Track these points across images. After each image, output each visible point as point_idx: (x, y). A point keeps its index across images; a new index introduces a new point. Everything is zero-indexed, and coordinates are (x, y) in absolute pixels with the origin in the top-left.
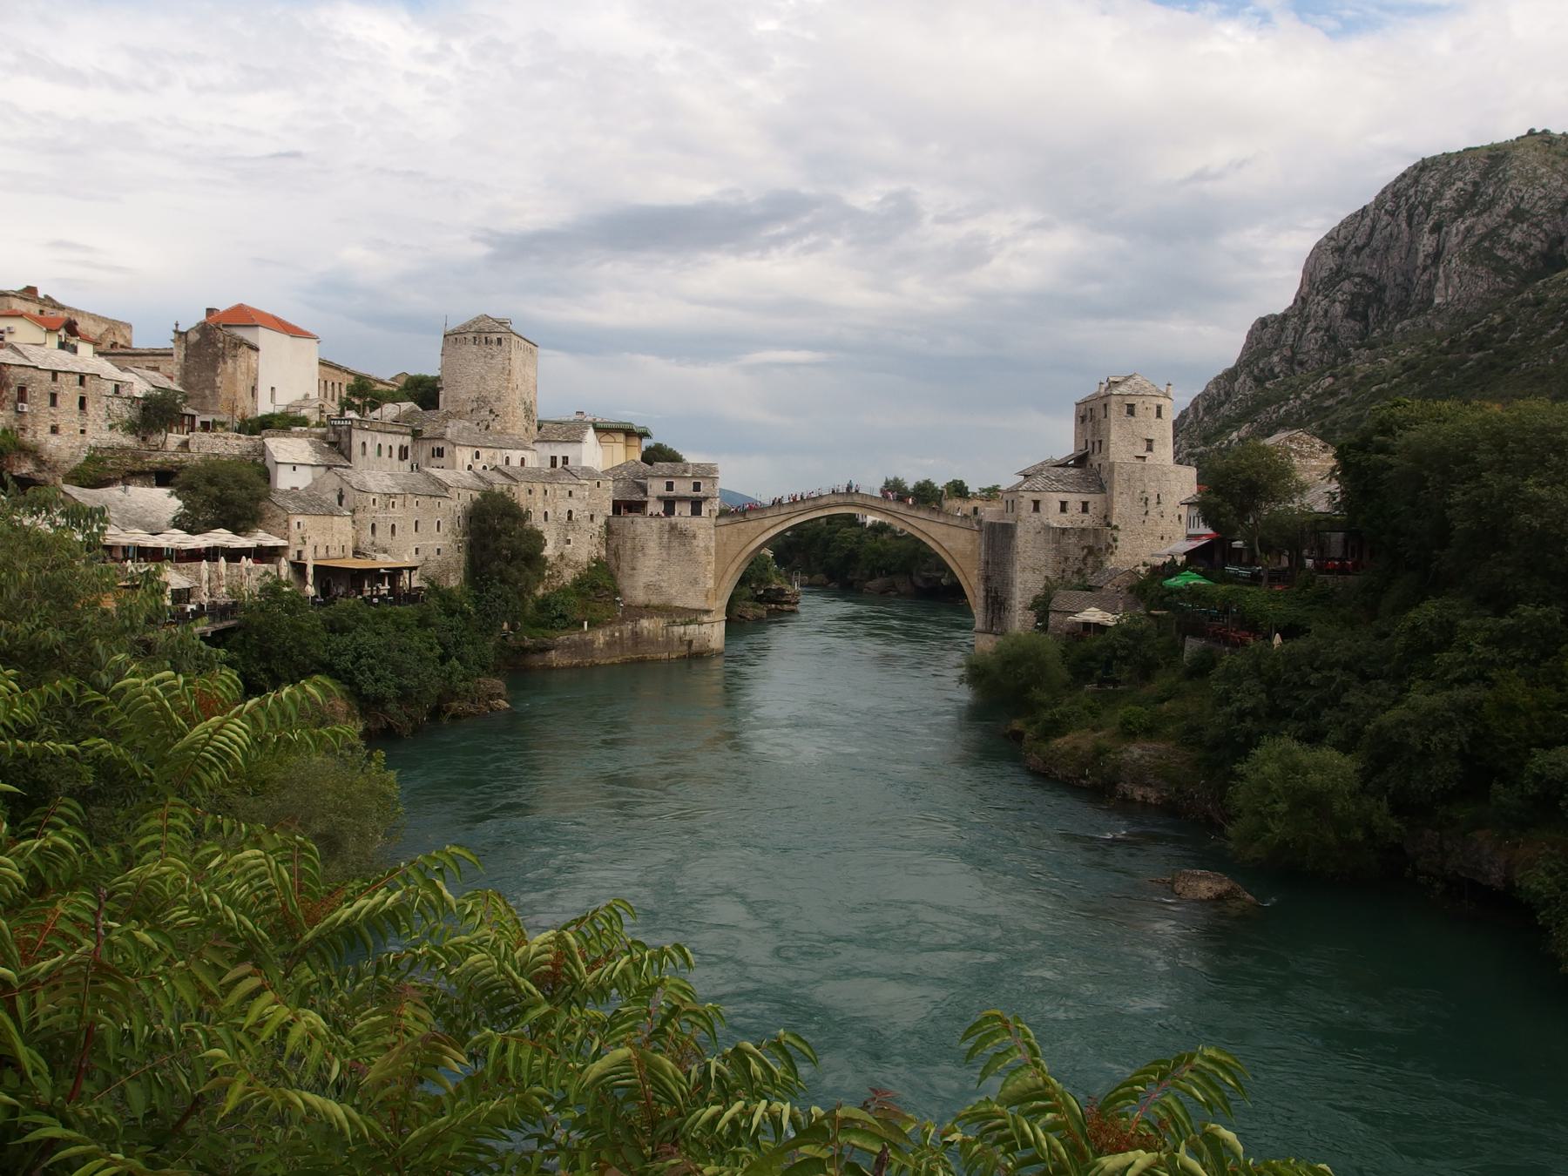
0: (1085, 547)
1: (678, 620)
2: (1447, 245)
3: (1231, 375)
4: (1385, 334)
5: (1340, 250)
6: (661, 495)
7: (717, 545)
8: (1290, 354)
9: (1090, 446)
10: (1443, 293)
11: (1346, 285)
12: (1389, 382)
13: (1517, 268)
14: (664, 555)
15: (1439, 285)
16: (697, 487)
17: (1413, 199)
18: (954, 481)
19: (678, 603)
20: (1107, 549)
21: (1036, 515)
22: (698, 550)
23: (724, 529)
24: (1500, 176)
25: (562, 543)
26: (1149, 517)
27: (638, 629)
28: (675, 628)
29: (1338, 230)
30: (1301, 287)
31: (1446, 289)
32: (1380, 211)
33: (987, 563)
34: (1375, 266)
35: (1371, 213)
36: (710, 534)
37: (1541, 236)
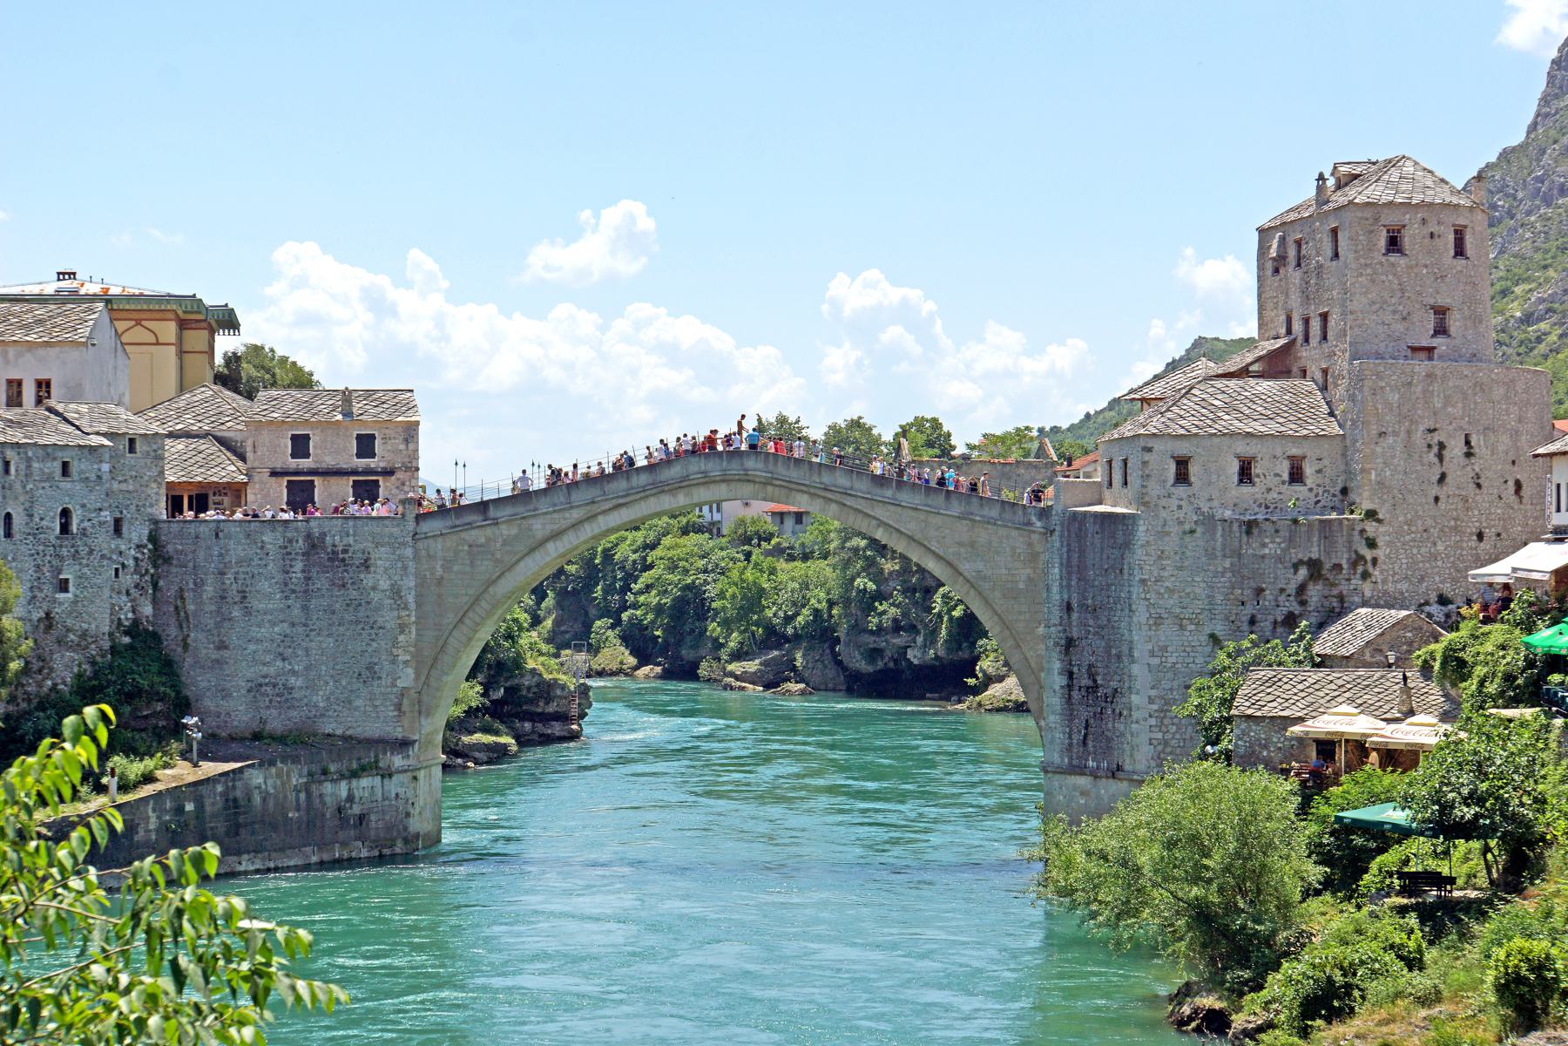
0: (1301, 562)
1: (332, 768)
6: (278, 465)
7: (422, 583)
9: (1297, 327)
14: (296, 611)
16: (366, 445)
18: (919, 423)
19: (329, 728)
20: (1354, 565)
21: (1181, 490)
22: (375, 597)
23: (438, 546)
25: (47, 589)
26: (1449, 488)
27: (238, 793)
28: (328, 788)
33: (1069, 608)
36: (400, 558)
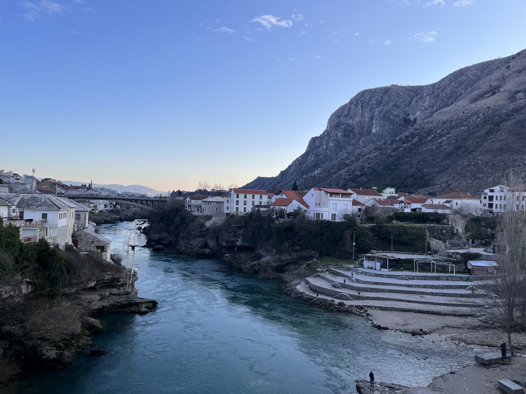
2: (375, 114)
3: (306, 154)
4: (356, 142)
5: (339, 117)
8: (325, 147)
10: (375, 129)
11: (342, 127)
12: (372, 154)
13: (397, 123)
15: (374, 126)
17: (362, 101)
24: (390, 94)
29: (338, 110)
30: (327, 127)
31: (376, 128)
32: (352, 104)
34: (351, 121)
35: (349, 105)
37: (403, 113)
